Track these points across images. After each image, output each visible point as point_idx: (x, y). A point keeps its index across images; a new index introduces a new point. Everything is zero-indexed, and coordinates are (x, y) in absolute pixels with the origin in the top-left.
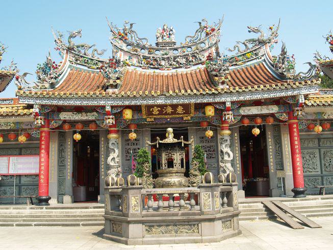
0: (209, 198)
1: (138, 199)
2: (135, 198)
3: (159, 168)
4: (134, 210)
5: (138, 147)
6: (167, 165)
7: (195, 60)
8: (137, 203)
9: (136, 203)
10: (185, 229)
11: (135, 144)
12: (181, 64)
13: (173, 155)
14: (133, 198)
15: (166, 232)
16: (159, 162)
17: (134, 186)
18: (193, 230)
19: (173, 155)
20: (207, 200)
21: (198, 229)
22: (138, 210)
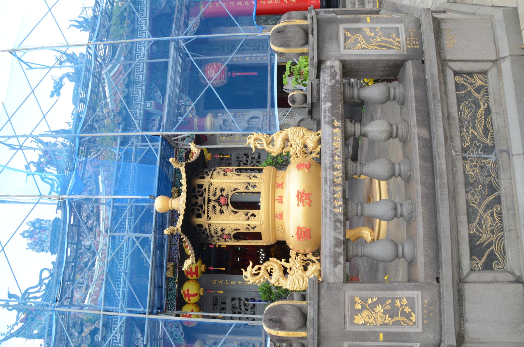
0: (358, 30)
1: (364, 300)
2: (360, 311)
3: (258, 236)
4: (408, 316)
5: (228, 301)
6: (251, 212)
7: (90, 186)
8: (381, 301)
9: (379, 309)
10: (474, 117)
11: (223, 306)
12: (92, 211)
13: (224, 193)
14: (359, 320)
15: (492, 188)
16: (239, 236)
17: (311, 313)
18: (478, 90)
19: (224, 193)
20: (367, 39)
21: (470, 74)
22: (411, 302)
